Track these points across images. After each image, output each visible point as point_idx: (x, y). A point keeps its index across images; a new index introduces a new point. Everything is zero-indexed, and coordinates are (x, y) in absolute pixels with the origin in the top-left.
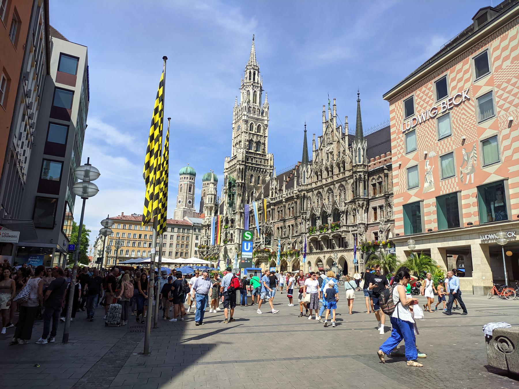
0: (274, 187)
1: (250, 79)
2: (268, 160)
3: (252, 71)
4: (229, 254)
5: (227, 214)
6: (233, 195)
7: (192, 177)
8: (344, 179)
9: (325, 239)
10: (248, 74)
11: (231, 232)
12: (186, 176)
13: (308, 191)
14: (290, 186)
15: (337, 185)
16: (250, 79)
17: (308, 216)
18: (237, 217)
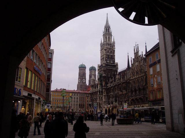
0: (118, 78)
1: (107, 31)
2: (115, 65)
3: (107, 28)
4: (101, 105)
5: (99, 89)
6: (102, 81)
7: (84, 69)
8: (142, 76)
9: (136, 99)
10: (106, 30)
11: (102, 96)
12: (82, 68)
13: (130, 80)
14: (123, 78)
15: (140, 78)
16: (107, 31)
17: (130, 90)
18: (104, 90)
